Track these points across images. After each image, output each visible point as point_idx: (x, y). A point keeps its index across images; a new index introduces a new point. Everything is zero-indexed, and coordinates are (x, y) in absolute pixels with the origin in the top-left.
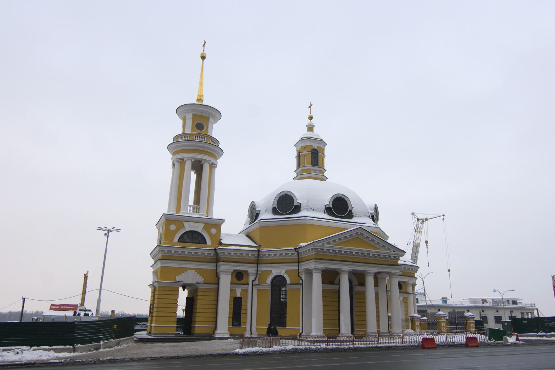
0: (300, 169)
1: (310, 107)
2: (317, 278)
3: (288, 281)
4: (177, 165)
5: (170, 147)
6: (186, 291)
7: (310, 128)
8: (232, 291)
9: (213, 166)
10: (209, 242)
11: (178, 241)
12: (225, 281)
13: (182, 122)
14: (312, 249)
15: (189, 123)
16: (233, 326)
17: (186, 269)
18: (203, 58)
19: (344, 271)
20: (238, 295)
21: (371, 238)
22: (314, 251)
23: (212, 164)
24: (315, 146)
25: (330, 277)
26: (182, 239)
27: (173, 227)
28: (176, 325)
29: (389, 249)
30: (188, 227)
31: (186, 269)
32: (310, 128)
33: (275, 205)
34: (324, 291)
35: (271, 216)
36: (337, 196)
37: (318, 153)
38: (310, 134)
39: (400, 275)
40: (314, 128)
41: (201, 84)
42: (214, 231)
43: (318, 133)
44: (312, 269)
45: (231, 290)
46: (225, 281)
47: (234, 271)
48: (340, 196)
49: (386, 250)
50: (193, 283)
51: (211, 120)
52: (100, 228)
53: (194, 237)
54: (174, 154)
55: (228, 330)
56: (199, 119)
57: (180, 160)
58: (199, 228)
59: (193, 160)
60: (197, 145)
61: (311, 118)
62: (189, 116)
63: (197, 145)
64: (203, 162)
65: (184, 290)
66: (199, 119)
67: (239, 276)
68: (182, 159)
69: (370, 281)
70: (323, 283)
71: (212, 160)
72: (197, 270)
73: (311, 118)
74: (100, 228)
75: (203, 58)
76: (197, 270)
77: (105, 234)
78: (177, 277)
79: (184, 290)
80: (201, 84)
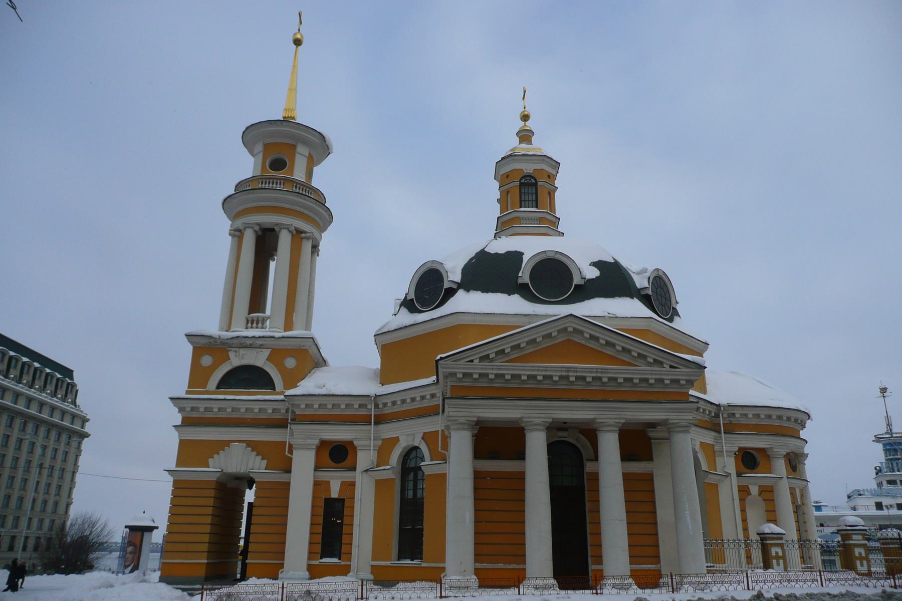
2: (461, 445)
7: (525, 136)
8: (319, 486)
11: (218, 387)
12: (304, 463)
17: (227, 443)
18: (298, 42)
21: (620, 344)
25: (497, 443)
26: (226, 382)
27: (207, 361)
28: (206, 561)
29: (657, 362)
30: (236, 360)
31: (227, 443)
32: (525, 136)
33: (412, 296)
34: (478, 476)
35: (406, 318)
36: (543, 257)
38: (524, 148)
39: (695, 425)
41: (292, 90)
43: (541, 144)
45: (316, 484)
46: (304, 463)
49: (649, 364)
53: (249, 377)
56: (284, 149)
57: (237, 233)
58: (259, 359)
60: (278, 204)
62: (259, 148)
63: (278, 204)
66: (284, 149)
67: (338, 454)
72: (250, 444)
73: (525, 118)
75: (298, 42)
76: (250, 444)
80: (292, 90)
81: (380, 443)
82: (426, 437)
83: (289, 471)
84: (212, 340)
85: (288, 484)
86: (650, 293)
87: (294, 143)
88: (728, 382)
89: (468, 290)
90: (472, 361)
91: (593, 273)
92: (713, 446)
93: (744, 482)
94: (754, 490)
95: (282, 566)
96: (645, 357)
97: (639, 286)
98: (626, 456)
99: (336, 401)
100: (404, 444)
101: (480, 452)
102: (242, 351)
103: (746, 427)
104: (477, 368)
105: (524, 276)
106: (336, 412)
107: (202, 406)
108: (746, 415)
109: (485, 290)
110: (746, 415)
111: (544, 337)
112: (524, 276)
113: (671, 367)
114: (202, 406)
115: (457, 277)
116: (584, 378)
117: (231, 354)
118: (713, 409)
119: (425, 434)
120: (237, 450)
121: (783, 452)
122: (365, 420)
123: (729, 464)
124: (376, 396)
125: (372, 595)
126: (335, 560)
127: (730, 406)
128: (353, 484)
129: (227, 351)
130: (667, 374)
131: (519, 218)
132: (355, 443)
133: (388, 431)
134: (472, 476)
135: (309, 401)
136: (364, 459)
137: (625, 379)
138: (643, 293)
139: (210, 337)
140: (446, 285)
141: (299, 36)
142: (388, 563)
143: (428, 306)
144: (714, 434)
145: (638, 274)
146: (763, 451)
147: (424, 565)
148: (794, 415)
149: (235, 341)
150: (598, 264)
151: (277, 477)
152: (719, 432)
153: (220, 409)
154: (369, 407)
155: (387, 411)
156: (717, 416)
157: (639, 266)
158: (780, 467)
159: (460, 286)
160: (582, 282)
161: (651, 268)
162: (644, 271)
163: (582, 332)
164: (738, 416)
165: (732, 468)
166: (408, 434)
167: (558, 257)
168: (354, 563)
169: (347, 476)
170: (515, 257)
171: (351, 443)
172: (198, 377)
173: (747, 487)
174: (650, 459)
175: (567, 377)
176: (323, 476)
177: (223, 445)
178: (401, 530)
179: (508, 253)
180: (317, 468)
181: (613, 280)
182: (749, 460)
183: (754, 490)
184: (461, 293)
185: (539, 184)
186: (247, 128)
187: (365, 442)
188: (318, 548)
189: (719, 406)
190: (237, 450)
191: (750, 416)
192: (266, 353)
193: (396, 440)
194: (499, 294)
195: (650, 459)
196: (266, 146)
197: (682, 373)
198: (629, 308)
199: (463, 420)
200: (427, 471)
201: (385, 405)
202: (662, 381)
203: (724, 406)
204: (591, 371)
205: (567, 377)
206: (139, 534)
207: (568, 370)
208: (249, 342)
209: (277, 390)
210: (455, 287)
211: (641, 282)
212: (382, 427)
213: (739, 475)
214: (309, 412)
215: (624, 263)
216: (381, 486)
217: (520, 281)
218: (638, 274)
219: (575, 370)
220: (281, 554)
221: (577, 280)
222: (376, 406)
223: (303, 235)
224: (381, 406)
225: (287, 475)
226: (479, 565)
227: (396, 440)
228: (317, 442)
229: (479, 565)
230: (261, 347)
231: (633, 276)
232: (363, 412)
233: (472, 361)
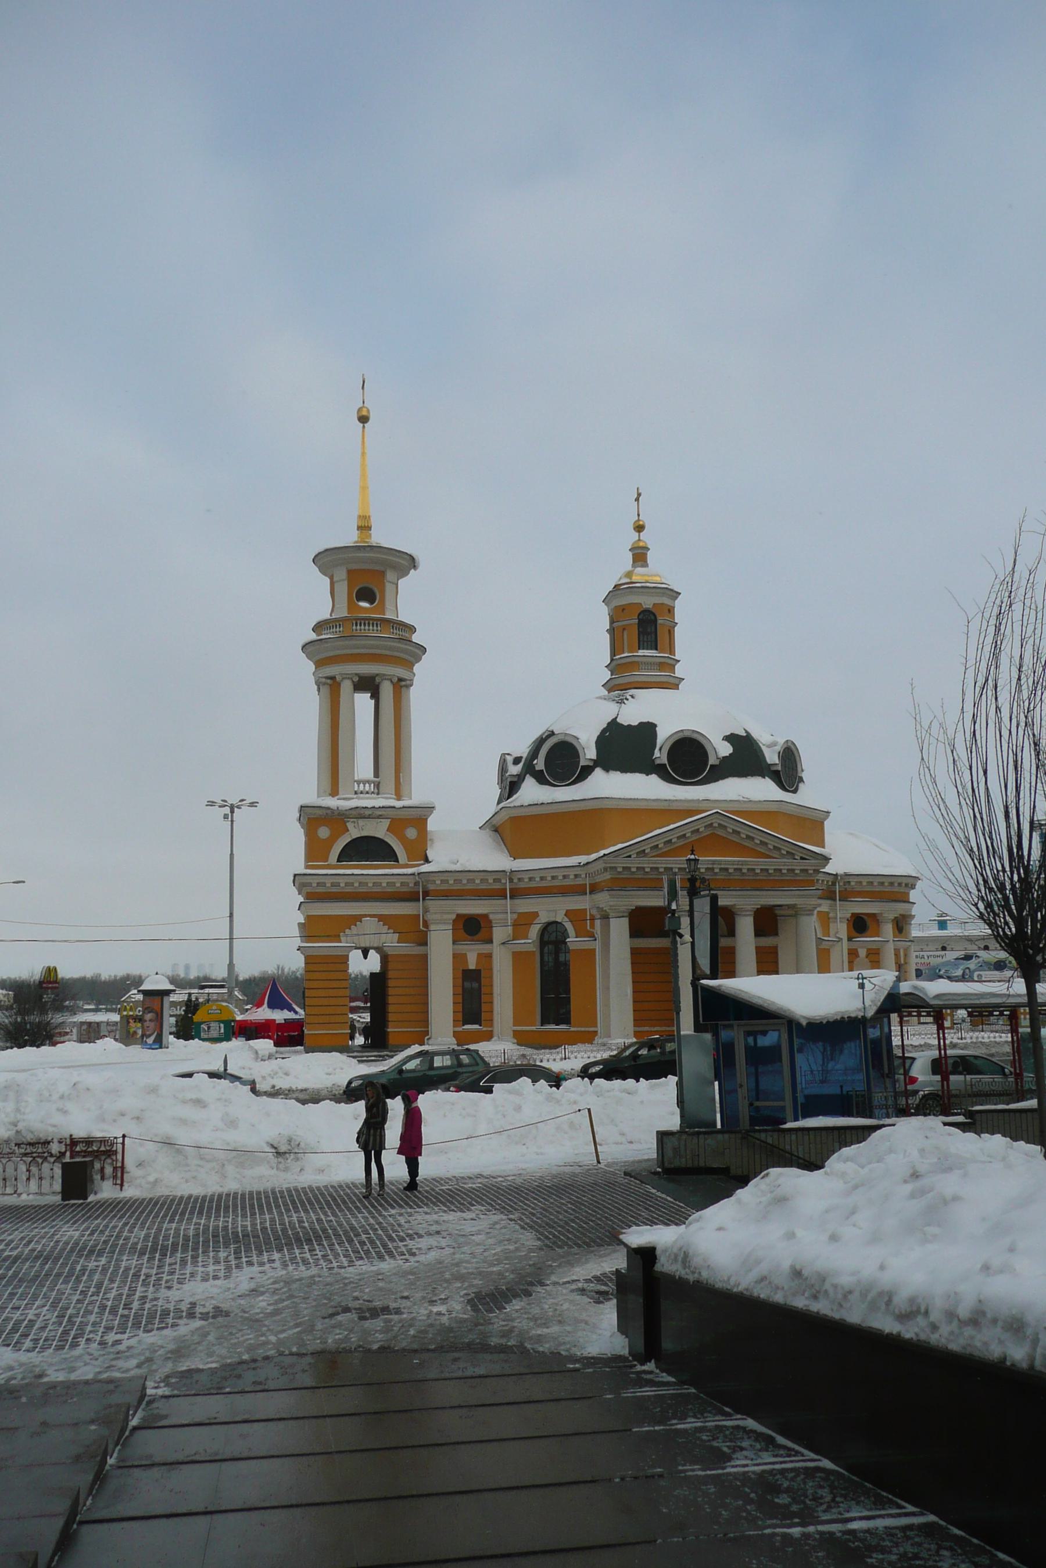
0: (614, 663)
1: (637, 500)
2: (619, 928)
4: (325, 690)
5: (310, 649)
7: (640, 556)
8: (458, 958)
9: (401, 685)
13: (328, 580)
15: (343, 588)
17: (357, 919)
18: (363, 419)
20: (472, 966)
23: (400, 680)
24: (648, 602)
27: (324, 832)
30: (354, 831)
31: (357, 919)
32: (640, 556)
37: (656, 620)
40: (650, 555)
42: (411, 833)
45: (455, 956)
48: (687, 734)
49: (783, 856)
51: (390, 575)
52: (211, 804)
54: (319, 664)
56: (365, 575)
57: (329, 681)
58: (379, 830)
59: (356, 679)
60: (364, 641)
61: (639, 528)
62: (341, 574)
63: (364, 641)
64: (378, 679)
66: (365, 575)
67: (472, 927)
68: (333, 678)
69: (745, 926)
71: (399, 672)
72: (381, 918)
73: (639, 528)
74: (211, 804)
75: (363, 419)
76: (381, 918)
77: (226, 817)
80: (364, 488)
81: (515, 916)
82: (568, 913)
83: (425, 944)
84: (329, 812)
85: (426, 956)
86: (779, 768)
87: (382, 569)
88: (848, 852)
89: (607, 769)
90: (630, 856)
91: (725, 750)
92: (828, 913)
93: (854, 946)
94: (862, 953)
95: (427, 1033)
96: (779, 849)
97: (769, 761)
98: (759, 933)
99: (471, 876)
100: (544, 918)
101: (635, 932)
102: (361, 822)
103: (860, 894)
104: (634, 864)
105: (660, 756)
106: (470, 887)
107: (328, 882)
108: (861, 882)
109: (625, 769)
110: (861, 882)
111: (693, 832)
112: (660, 756)
113: (802, 858)
114: (328, 882)
115: (590, 753)
116: (727, 869)
117: (350, 825)
118: (831, 879)
119: (567, 911)
120: (370, 925)
121: (892, 917)
122: (501, 894)
123: (841, 929)
124: (512, 871)
125: (572, 1056)
126: (477, 1027)
127: (846, 875)
128: (489, 956)
129: (345, 823)
130: (798, 865)
131: (638, 662)
132: (491, 917)
133: (525, 905)
134: (628, 955)
135: (444, 877)
136: (500, 934)
137: (762, 870)
138: (775, 768)
139: (328, 808)
140: (583, 763)
141: (364, 413)
142: (534, 1028)
143: (563, 780)
144: (829, 902)
145: (769, 746)
146: (873, 916)
147: (572, 1029)
148: (904, 881)
149: (354, 812)
150: (731, 738)
151: (418, 950)
152: (835, 900)
153: (347, 884)
154: (503, 881)
155: (522, 885)
156: (834, 884)
157: (770, 743)
158: (888, 929)
159: (597, 763)
160: (717, 762)
161: (781, 741)
162: (774, 744)
163: (725, 827)
164: (853, 884)
165: (843, 934)
166: (551, 910)
167: (695, 736)
168: (497, 1028)
169: (484, 948)
170: (648, 730)
171: (486, 916)
172: (315, 851)
173: (856, 950)
174: (776, 934)
175: (713, 869)
176: (462, 948)
177: (356, 919)
178: (543, 999)
179: (641, 723)
180: (454, 942)
181: (746, 757)
182: (860, 925)
183: (862, 953)
184: (598, 772)
185: (659, 622)
186: (327, 550)
187: (501, 914)
188: (460, 1016)
189: (836, 875)
190: (370, 925)
191: (864, 884)
192: (386, 823)
193: (536, 915)
194: (637, 774)
195: (776, 934)
196: (350, 573)
197: (810, 864)
198: (760, 790)
199: (622, 909)
200: (572, 947)
201: (520, 880)
202: (793, 870)
203: (841, 876)
204: (733, 863)
205: (713, 869)
206: (157, 999)
207: (714, 862)
208: (367, 812)
209: (401, 862)
210: (591, 764)
211: (772, 757)
212: (517, 901)
213: (850, 939)
214: (445, 887)
215: (755, 735)
216: (518, 958)
217: (658, 762)
218: (769, 746)
219: (720, 862)
220: (425, 1022)
221: (712, 760)
222: (511, 880)
223: (403, 683)
224: (515, 881)
225: (422, 948)
226: (637, 1029)
227: (536, 915)
228: (454, 917)
229: (637, 1029)
230: (380, 817)
231: (764, 748)
232: (497, 886)
233: (630, 856)
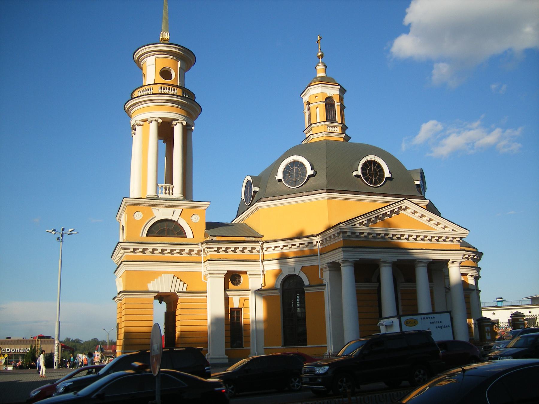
3: (306, 282)
6: (164, 304)
10: (189, 234)
14: (339, 233)
16: (232, 347)
19: (384, 262)
20: (236, 305)
22: (341, 235)
44: (340, 261)
47: (229, 272)
50: (172, 291)
55: (226, 354)
57: (142, 123)
59: (160, 121)
64: (174, 122)
65: (161, 302)
70: (357, 281)
78: (149, 285)
79: (161, 302)
